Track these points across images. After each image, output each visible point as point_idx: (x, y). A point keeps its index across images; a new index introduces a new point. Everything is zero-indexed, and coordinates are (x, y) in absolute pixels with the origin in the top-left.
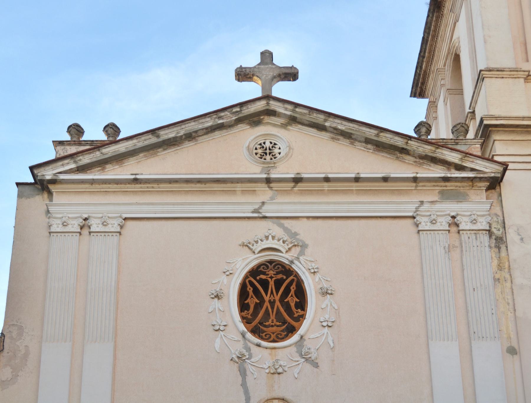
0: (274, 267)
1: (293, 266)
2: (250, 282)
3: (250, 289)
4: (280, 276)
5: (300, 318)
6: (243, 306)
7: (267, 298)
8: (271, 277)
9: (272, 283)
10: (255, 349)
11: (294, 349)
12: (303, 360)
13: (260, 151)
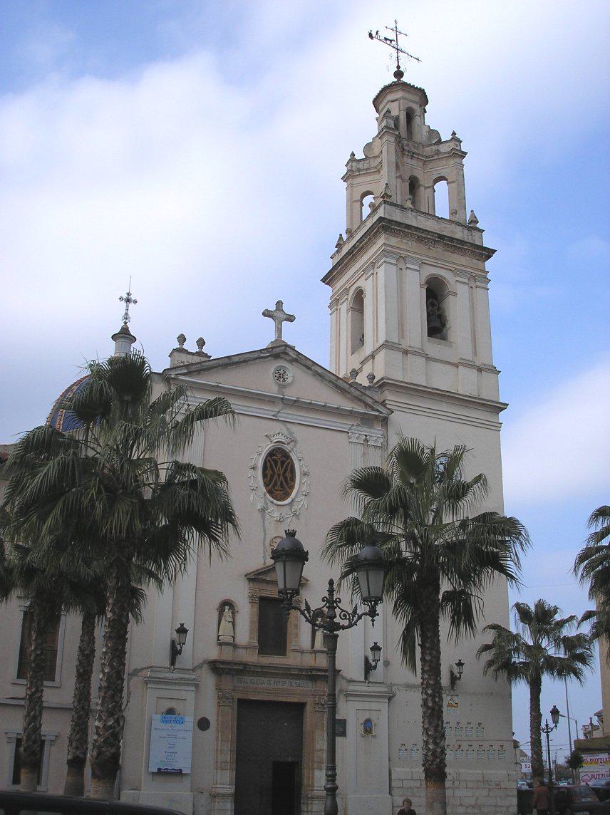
4: (283, 459)
6: (265, 476)
9: (279, 464)
13: (277, 375)
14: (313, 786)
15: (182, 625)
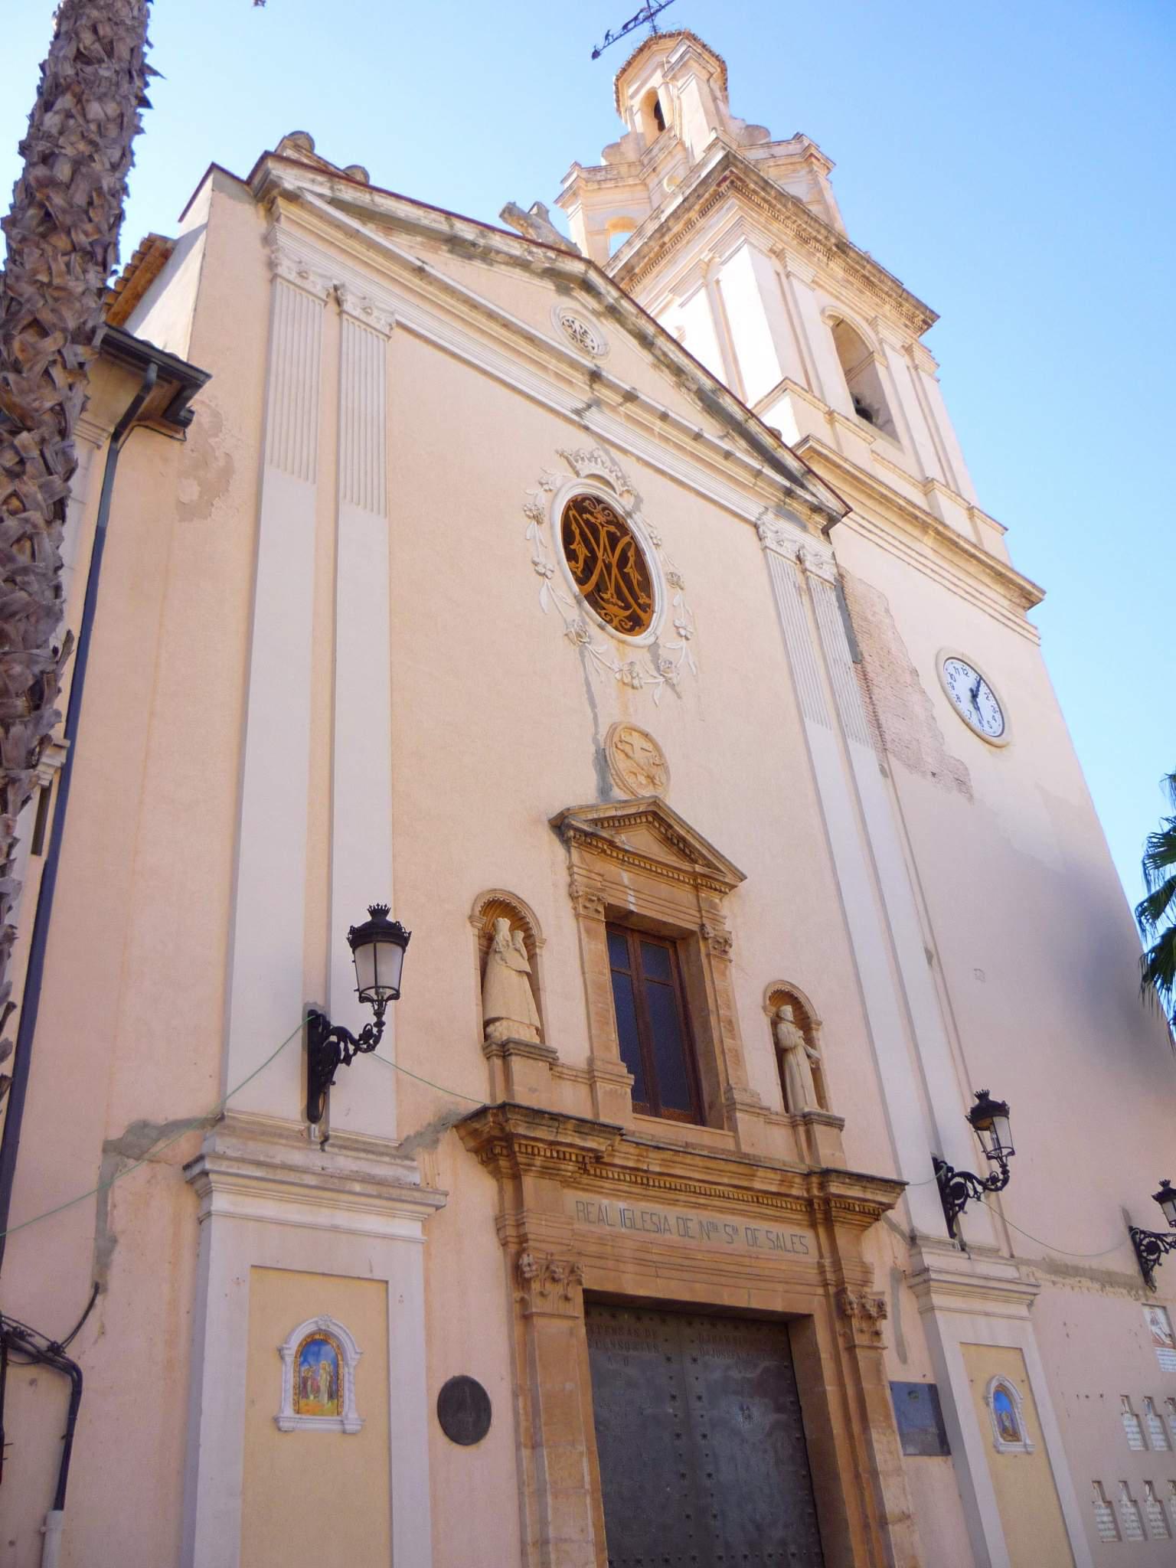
1: (629, 521)
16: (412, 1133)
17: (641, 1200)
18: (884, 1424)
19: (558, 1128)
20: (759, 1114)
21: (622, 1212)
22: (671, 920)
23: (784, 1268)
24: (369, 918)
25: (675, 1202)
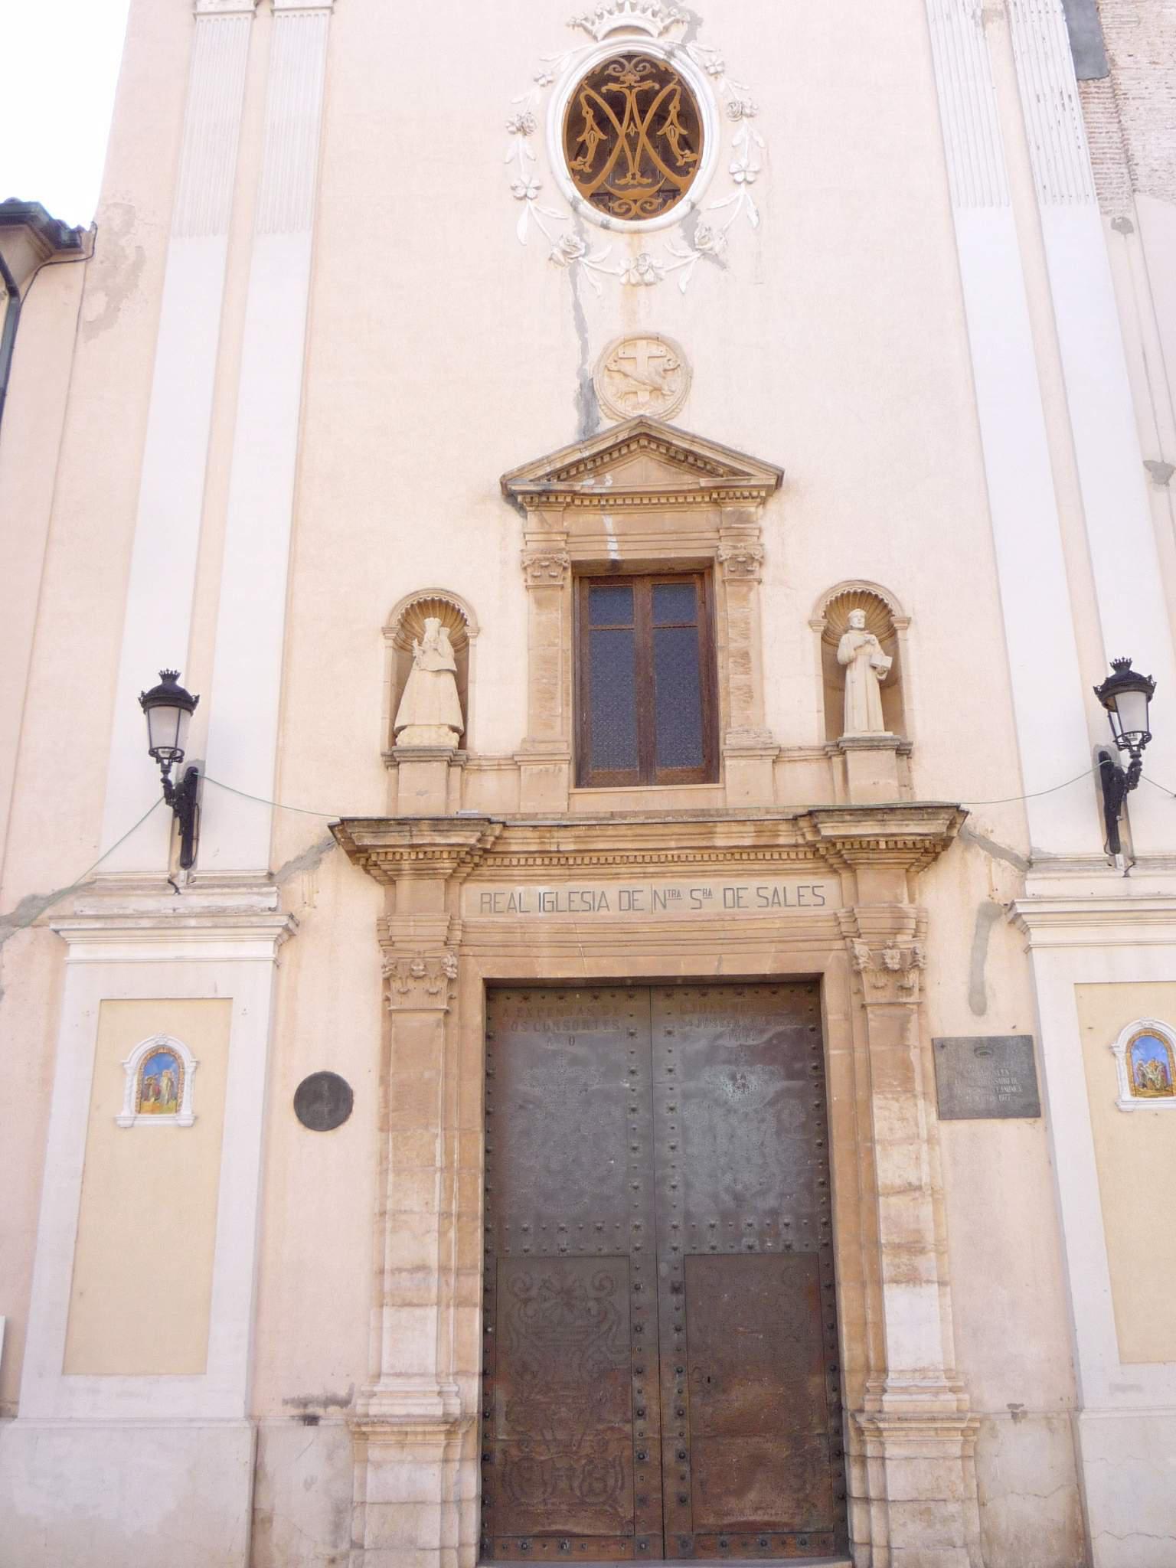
0: (636, 66)
1: (672, 63)
2: (589, 100)
3: (588, 114)
4: (648, 85)
5: (688, 170)
6: (574, 148)
7: (621, 130)
8: (630, 88)
9: (631, 102)
10: (595, 234)
11: (678, 232)
12: (697, 254)
14: (884, 1370)
15: (169, 677)
16: (292, 859)
17: (569, 880)
18: (899, 1089)
19: (411, 831)
20: (761, 756)
21: (541, 898)
22: (673, 555)
23: (778, 926)
24: (159, 682)
25: (617, 876)
